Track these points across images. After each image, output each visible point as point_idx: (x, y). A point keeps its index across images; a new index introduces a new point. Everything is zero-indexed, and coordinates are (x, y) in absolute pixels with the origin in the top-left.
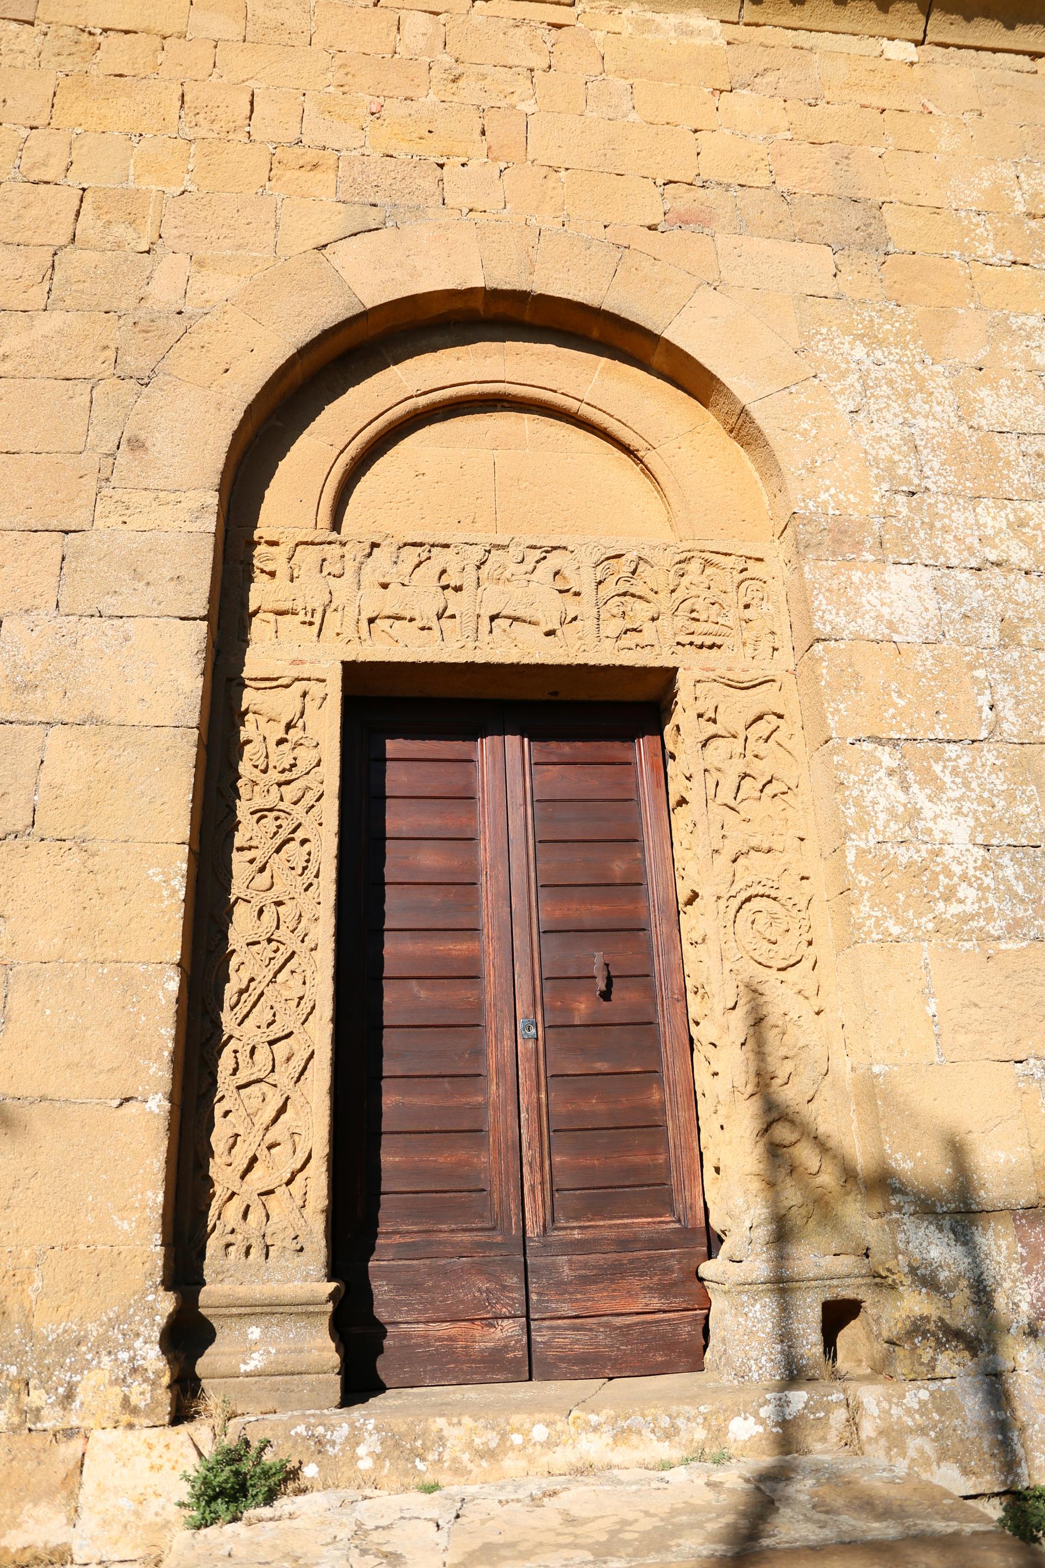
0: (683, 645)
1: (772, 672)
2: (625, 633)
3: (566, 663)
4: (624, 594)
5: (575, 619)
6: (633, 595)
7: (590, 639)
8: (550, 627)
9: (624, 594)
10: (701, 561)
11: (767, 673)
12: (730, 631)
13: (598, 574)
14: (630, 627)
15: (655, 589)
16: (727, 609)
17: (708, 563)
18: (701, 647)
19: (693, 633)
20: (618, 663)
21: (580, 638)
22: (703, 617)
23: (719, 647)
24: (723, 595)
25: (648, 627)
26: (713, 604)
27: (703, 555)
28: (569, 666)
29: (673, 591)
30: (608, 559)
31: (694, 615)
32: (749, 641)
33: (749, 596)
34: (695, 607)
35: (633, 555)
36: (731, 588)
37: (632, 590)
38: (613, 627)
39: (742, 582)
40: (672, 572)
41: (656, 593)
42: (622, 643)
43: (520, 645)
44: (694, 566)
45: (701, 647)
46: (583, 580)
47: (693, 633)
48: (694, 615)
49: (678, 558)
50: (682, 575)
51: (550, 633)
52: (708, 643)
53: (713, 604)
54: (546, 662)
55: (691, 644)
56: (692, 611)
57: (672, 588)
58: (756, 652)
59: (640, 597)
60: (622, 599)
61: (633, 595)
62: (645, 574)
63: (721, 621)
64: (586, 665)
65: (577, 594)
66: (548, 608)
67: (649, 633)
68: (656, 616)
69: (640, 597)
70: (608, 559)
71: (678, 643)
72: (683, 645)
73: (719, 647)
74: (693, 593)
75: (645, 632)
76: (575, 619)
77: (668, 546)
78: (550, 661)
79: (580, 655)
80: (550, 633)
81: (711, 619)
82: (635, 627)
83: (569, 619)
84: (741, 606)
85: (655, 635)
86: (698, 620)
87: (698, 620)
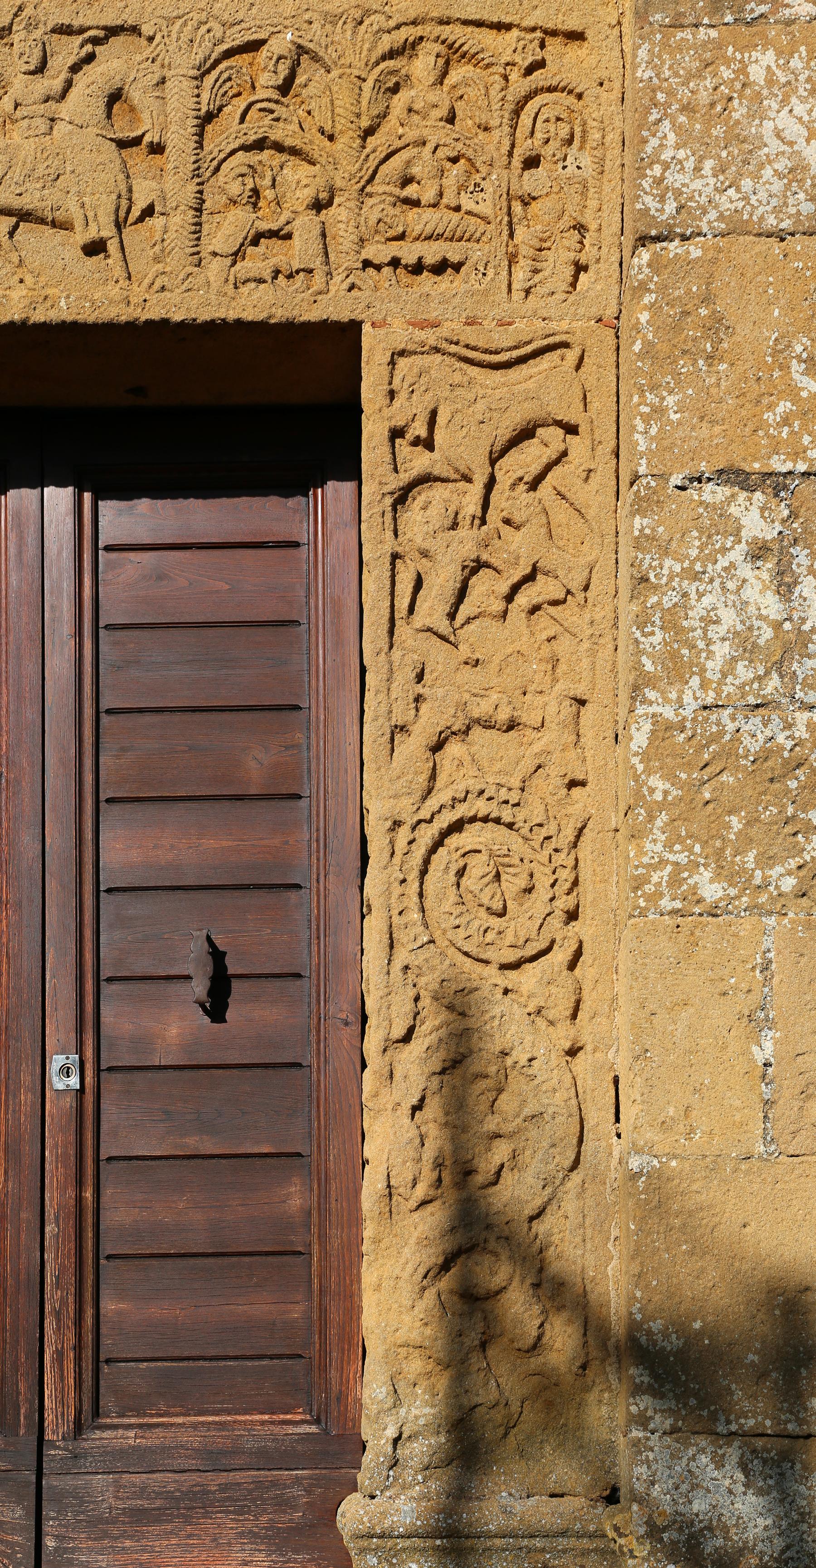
0: (378, 268)
1: (564, 325)
2: (255, 242)
3: (123, 318)
4: (260, 145)
5: (149, 211)
6: (279, 147)
7: (178, 260)
8: (92, 233)
9: (260, 145)
10: (438, 48)
11: (554, 326)
12: (482, 227)
13: (205, 96)
14: (264, 226)
15: (328, 128)
16: (484, 170)
17: (453, 55)
18: (417, 268)
19: (401, 237)
20: (232, 315)
21: (157, 260)
22: (429, 196)
23: (457, 267)
24: (482, 135)
25: (305, 226)
26: (454, 160)
27: (446, 31)
28: (131, 326)
29: (370, 132)
30: (229, 54)
31: (411, 191)
32: (524, 250)
33: (539, 135)
34: (416, 170)
35: (281, 44)
36: (498, 118)
37: (276, 135)
38: (227, 228)
39: (528, 98)
40: (370, 82)
41: (331, 138)
42: (244, 268)
43: (29, 280)
44: (422, 66)
45: (417, 268)
46: (169, 114)
47: (401, 237)
48: (411, 191)
49: (386, 43)
50: (395, 90)
51: (95, 248)
52: (430, 260)
53: (454, 160)
54: (81, 318)
55: (395, 263)
56: (407, 181)
57: (365, 123)
58: (537, 278)
59: (294, 152)
60: (254, 158)
61: (279, 147)
62: (311, 90)
63: (467, 203)
64: (165, 322)
65: (157, 149)
66: (89, 185)
67: (302, 249)
68: (323, 196)
69: (294, 152)
70: (229, 54)
71: (367, 264)
72: (378, 268)
73: (457, 267)
74: (411, 135)
75: (296, 240)
76: (149, 211)
77: (368, 13)
78: (89, 316)
79: (154, 298)
80: (95, 248)
81: (445, 201)
82: (274, 226)
83: (136, 213)
84: (517, 162)
85: (317, 246)
86: (416, 203)
87: (416, 203)
